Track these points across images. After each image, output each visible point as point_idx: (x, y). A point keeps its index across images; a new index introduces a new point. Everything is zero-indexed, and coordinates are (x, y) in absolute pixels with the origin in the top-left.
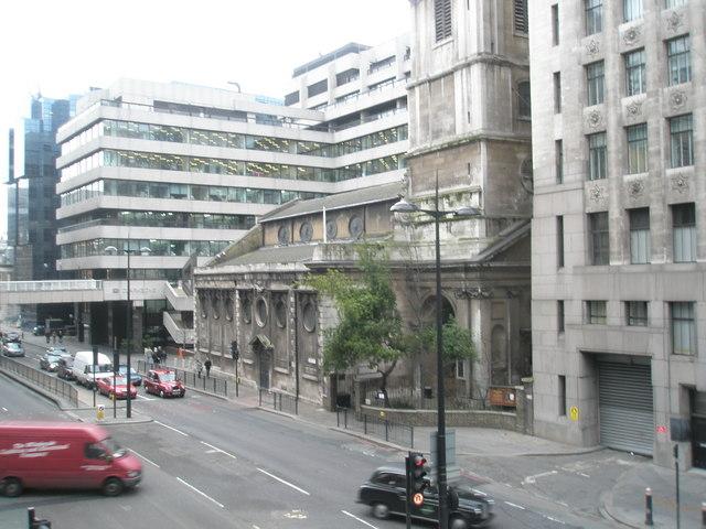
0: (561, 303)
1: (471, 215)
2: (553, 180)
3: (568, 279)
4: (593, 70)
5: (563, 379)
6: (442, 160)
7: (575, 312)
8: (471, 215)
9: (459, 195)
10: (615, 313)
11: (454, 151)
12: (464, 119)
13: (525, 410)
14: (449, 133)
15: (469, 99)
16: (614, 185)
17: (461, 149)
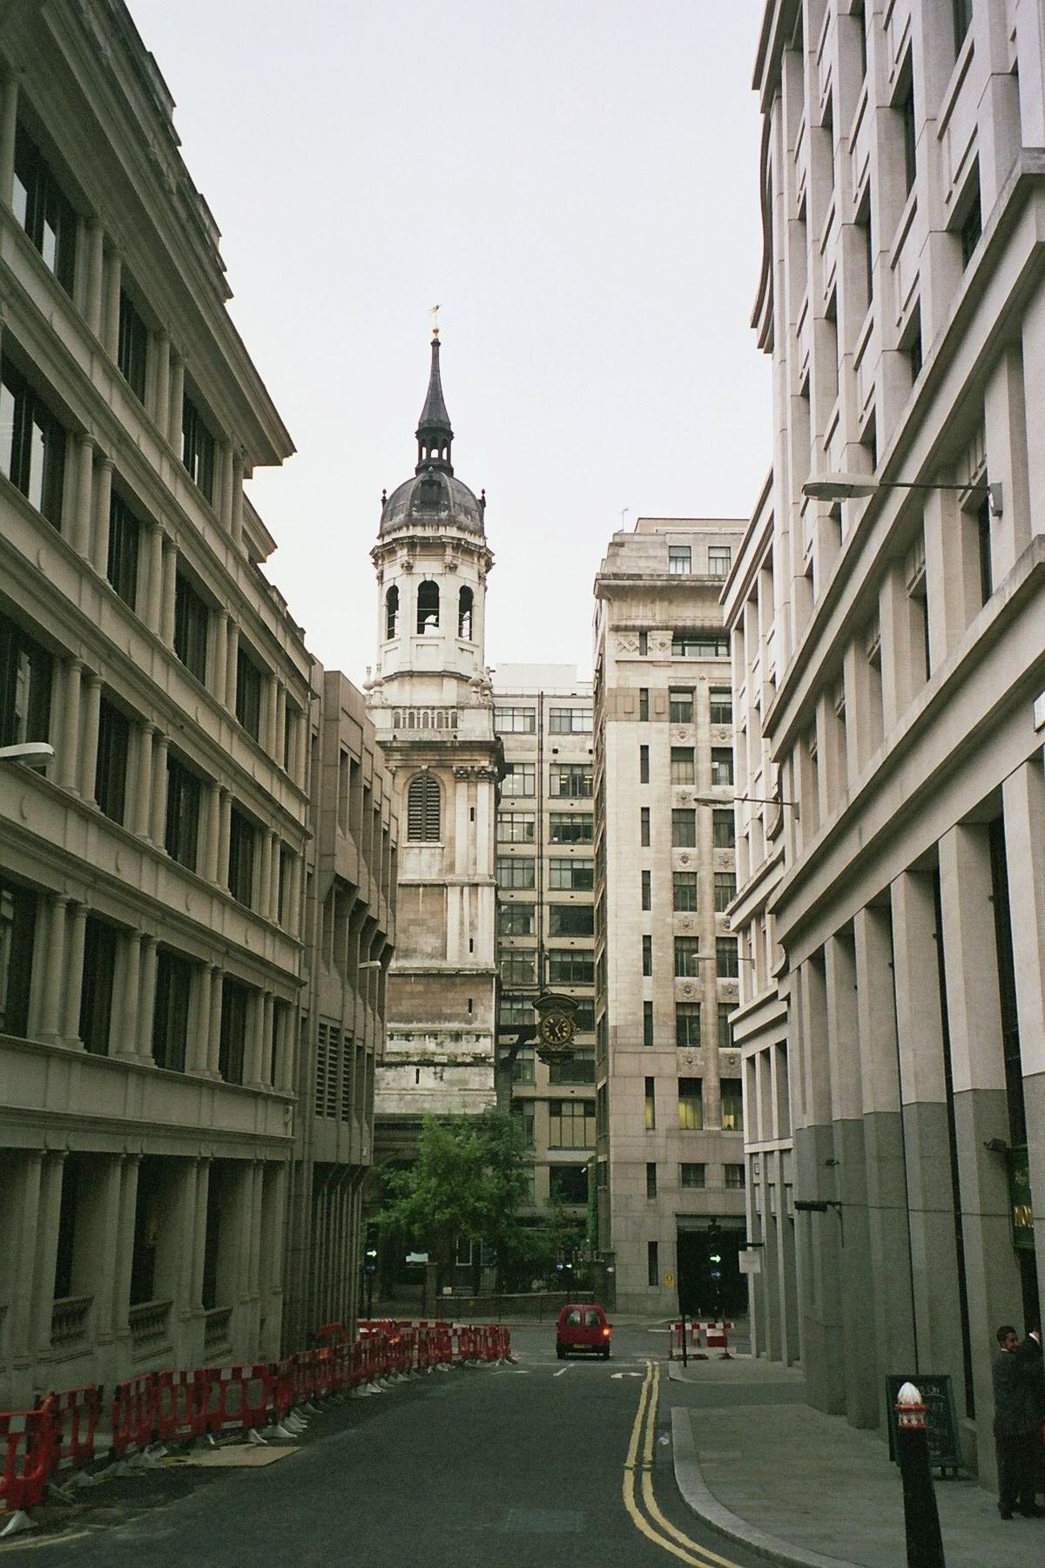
0: (651, 1168)
1: (479, 1061)
2: (642, 1041)
3: (660, 1141)
4: (685, 945)
5: (653, 1247)
6: (420, 988)
7: (668, 1175)
8: (479, 1061)
9: (457, 1036)
10: (715, 1176)
11: (443, 981)
12: (461, 945)
13: (604, 1287)
14: (431, 956)
15: (471, 924)
16: (711, 1054)
17: (458, 980)
